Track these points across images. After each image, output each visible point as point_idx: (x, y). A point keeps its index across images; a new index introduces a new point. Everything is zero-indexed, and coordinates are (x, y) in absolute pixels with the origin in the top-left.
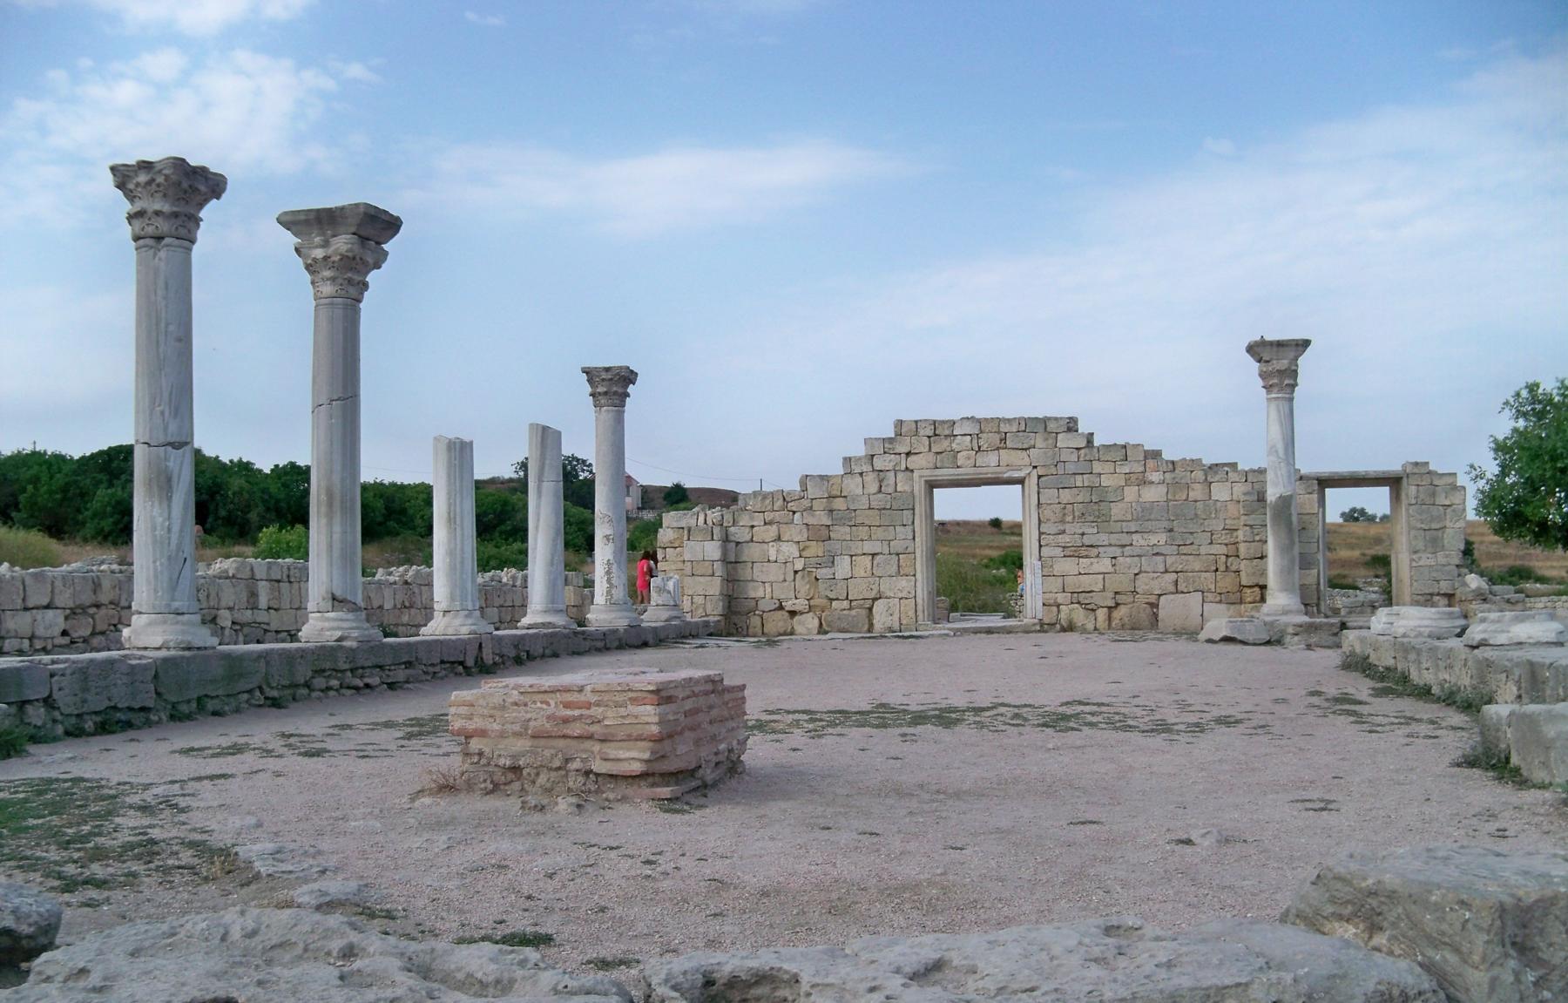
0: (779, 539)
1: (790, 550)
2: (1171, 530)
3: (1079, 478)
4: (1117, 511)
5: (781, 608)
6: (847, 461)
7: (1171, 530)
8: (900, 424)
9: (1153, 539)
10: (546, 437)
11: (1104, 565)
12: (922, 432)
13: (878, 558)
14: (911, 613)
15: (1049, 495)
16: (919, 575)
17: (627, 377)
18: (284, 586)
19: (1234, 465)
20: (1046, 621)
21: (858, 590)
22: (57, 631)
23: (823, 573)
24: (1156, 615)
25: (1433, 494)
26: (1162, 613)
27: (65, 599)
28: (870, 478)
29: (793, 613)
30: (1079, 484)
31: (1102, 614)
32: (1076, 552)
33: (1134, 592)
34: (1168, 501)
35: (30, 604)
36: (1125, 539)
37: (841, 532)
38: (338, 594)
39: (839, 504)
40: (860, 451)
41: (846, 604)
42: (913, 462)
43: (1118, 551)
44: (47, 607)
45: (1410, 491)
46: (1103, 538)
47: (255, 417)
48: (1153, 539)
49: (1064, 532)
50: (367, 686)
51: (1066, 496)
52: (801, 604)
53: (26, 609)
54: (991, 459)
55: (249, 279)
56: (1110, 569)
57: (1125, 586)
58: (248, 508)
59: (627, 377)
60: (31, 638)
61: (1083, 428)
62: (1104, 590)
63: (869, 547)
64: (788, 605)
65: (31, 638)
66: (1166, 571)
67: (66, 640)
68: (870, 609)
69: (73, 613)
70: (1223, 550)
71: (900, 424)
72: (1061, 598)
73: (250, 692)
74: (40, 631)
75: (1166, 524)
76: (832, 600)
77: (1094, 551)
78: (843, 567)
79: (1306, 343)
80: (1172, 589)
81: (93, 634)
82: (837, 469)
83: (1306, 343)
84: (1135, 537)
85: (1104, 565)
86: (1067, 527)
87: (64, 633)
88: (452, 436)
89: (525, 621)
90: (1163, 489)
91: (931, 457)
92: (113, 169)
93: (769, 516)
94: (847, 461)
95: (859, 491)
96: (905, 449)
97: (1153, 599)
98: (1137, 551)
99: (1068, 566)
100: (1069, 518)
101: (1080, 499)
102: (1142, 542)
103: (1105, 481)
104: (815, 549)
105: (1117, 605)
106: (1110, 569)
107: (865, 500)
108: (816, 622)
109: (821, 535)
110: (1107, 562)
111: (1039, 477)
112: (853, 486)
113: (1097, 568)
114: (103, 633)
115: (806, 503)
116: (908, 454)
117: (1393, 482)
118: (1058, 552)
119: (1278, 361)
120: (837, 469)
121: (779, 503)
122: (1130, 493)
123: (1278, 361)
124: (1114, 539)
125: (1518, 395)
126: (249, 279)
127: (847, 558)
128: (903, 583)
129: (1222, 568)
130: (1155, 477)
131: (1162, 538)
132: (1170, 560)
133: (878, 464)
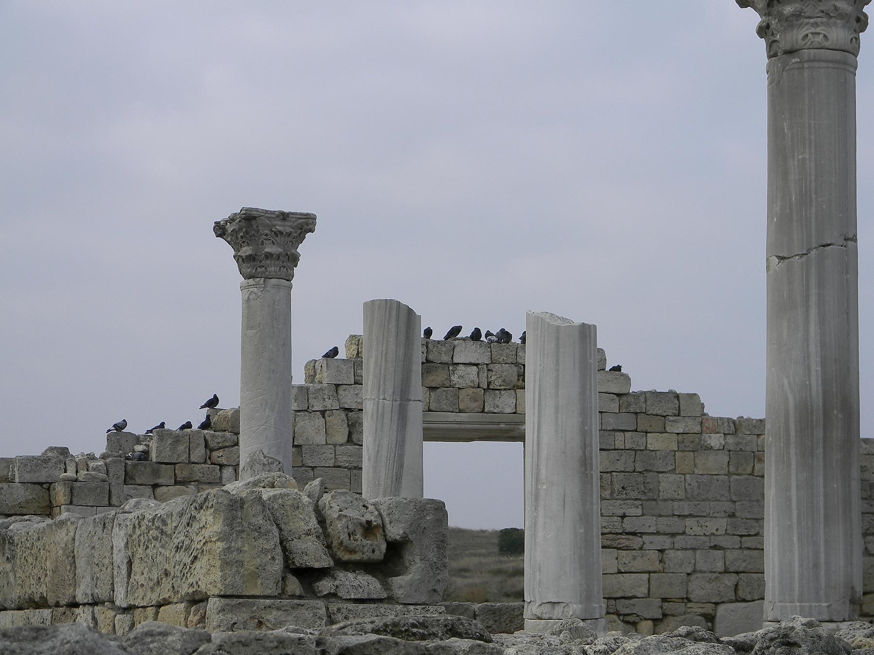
2: (732, 515)
4: (667, 484)
7: (732, 515)
9: (712, 526)
11: (650, 560)
28: (338, 421)
30: (619, 444)
34: (729, 474)
36: (676, 525)
43: (664, 542)
46: (649, 523)
48: (712, 526)
56: (658, 566)
57: (676, 592)
62: (649, 596)
66: (726, 571)
75: (727, 506)
77: (636, 542)
80: (731, 595)
84: (689, 522)
85: (650, 560)
88: (538, 310)
90: (724, 458)
95: (320, 439)
97: (708, 609)
98: (691, 542)
101: (620, 466)
102: (697, 530)
103: (655, 442)
105: (665, 615)
106: (658, 566)
107: (329, 452)
110: (655, 556)
113: (638, 565)
121: (199, 453)
124: (664, 524)
125: (335, 352)
130: (715, 440)
131: (720, 524)
132: (731, 555)
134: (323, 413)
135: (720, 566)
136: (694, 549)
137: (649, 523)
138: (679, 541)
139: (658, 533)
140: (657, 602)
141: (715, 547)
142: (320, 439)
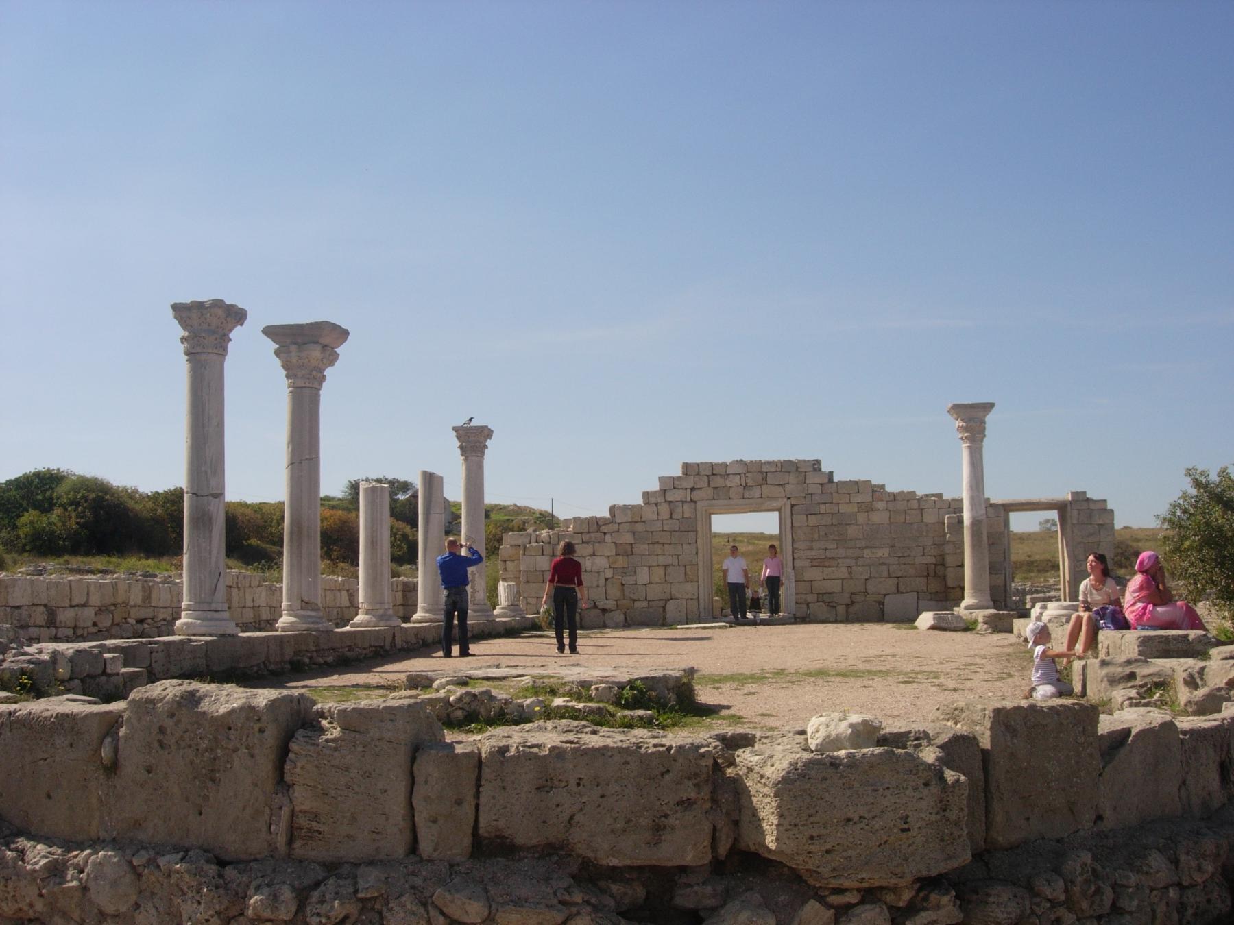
0: (594, 554)
1: (601, 562)
3: (822, 507)
4: (852, 531)
5: (595, 607)
6: (646, 495)
8: (686, 467)
9: (879, 553)
10: (431, 480)
11: (843, 573)
12: (703, 473)
13: (670, 569)
14: (695, 610)
15: (800, 520)
16: (701, 580)
17: (485, 433)
18: (235, 591)
19: (940, 496)
20: (799, 615)
21: (655, 592)
22: (90, 624)
23: (628, 580)
24: (882, 611)
25: (1090, 516)
26: (887, 609)
27: (95, 600)
28: (665, 509)
29: (604, 611)
31: (841, 609)
32: (819, 563)
33: (866, 593)
34: (891, 523)
35: (74, 603)
37: (641, 548)
38: (306, 599)
39: (640, 528)
40: (655, 486)
41: (645, 604)
42: (697, 495)
43: (852, 562)
44: (84, 605)
45: (1073, 513)
46: (842, 552)
47: (255, 476)
48: (879, 553)
49: (811, 549)
50: (326, 663)
51: (813, 520)
52: (610, 604)
53: (72, 607)
54: (756, 492)
55: (255, 381)
56: (847, 575)
58: (251, 538)
59: (485, 433)
60: (75, 628)
61: (825, 468)
63: (662, 560)
64: (601, 605)
65: (75, 628)
67: (94, 630)
68: (664, 608)
69: (101, 610)
70: (933, 560)
71: (686, 467)
72: (810, 598)
73: (258, 665)
74: (81, 624)
76: (634, 600)
77: (834, 563)
78: (642, 576)
79: (992, 405)
80: (894, 589)
81: (113, 624)
82: (638, 501)
83: (992, 405)
84: (866, 551)
85: (843, 573)
86: (815, 545)
87: (95, 624)
89: (415, 617)
91: (710, 491)
92: (180, 311)
93: (586, 538)
94: (646, 495)
95: (655, 517)
96: (691, 485)
97: (880, 598)
99: (813, 574)
100: (816, 536)
101: (823, 522)
103: (843, 508)
104: (621, 562)
105: (853, 602)
108: (622, 617)
109: (625, 551)
110: (845, 570)
111: (792, 506)
112: (650, 514)
114: (118, 624)
115: (615, 527)
116: (692, 489)
117: (1061, 507)
118: (807, 563)
119: (973, 419)
120: (640, 502)
122: (861, 518)
123: (973, 419)
126: (255, 381)
127: (646, 569)
128: (689, 587)
129: (932, 573)
130: (880, 505)
131: (884, 552)
133: (670, 497)
134: (656, 505)
135: (885, 574)
136: (869, 565)
137: (842, 553)
138: (860, 562)
139: (846, 558)
140: (848, 595)
141: (883, 564)
142: (655, 517)
